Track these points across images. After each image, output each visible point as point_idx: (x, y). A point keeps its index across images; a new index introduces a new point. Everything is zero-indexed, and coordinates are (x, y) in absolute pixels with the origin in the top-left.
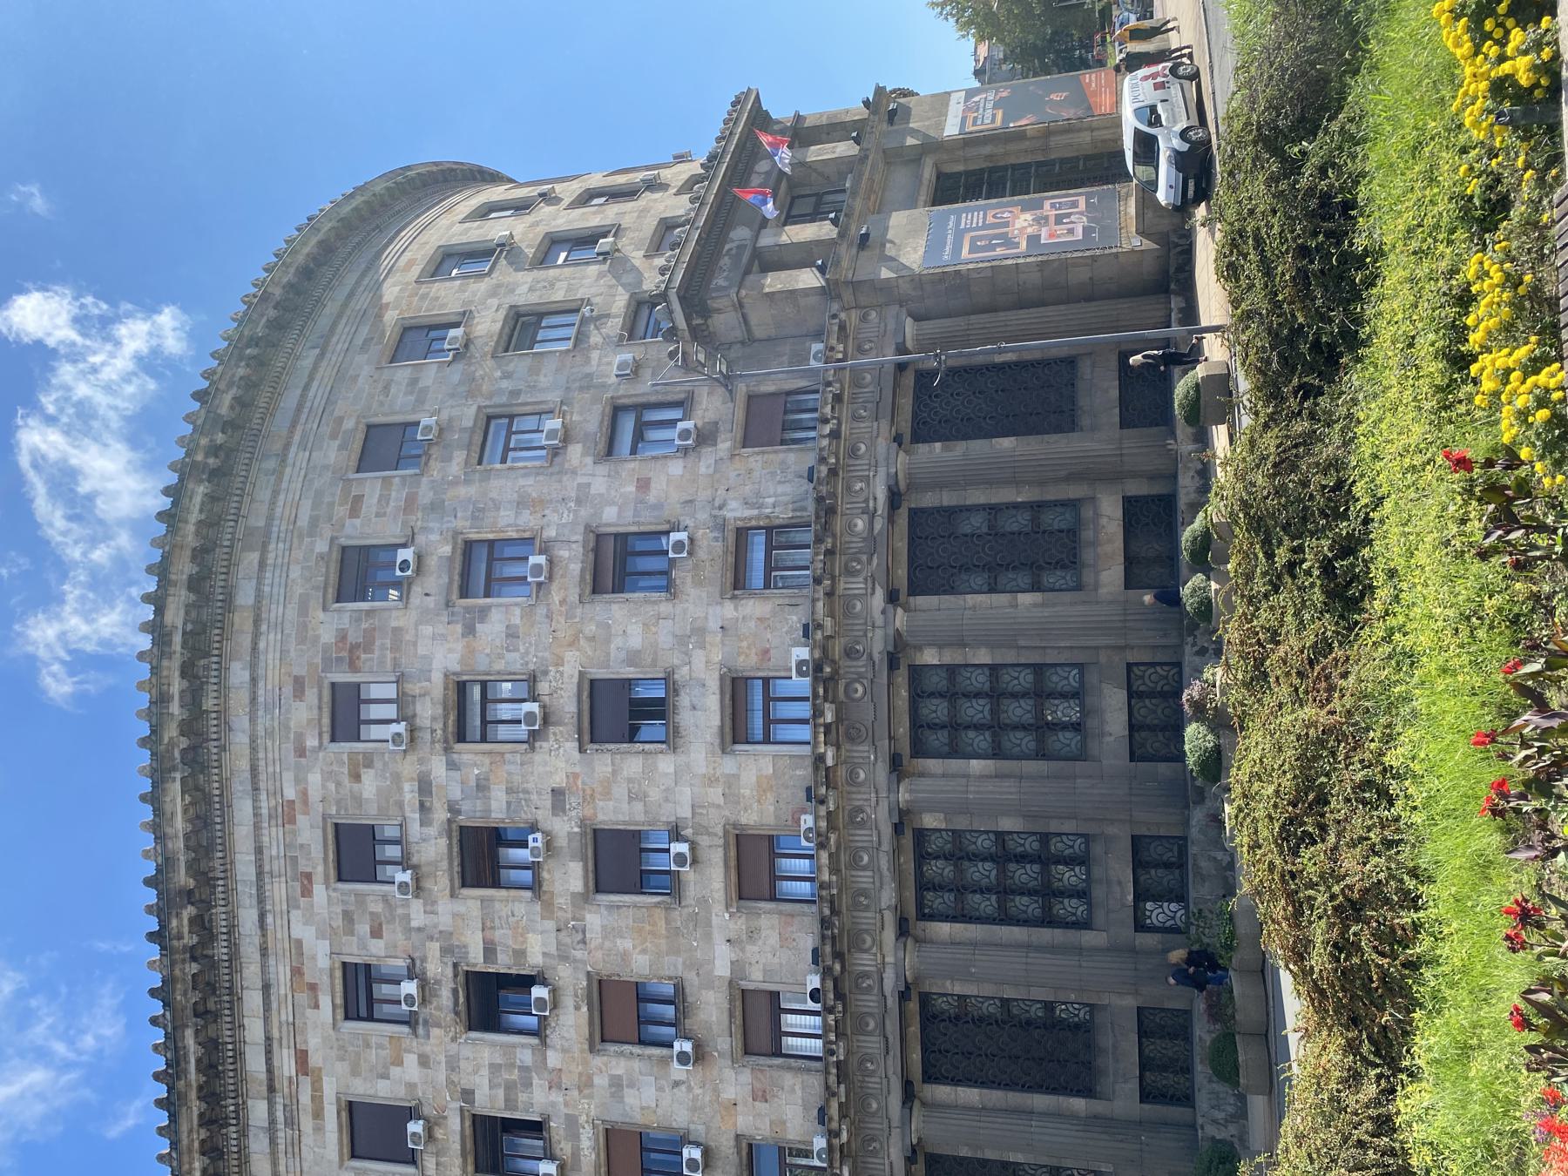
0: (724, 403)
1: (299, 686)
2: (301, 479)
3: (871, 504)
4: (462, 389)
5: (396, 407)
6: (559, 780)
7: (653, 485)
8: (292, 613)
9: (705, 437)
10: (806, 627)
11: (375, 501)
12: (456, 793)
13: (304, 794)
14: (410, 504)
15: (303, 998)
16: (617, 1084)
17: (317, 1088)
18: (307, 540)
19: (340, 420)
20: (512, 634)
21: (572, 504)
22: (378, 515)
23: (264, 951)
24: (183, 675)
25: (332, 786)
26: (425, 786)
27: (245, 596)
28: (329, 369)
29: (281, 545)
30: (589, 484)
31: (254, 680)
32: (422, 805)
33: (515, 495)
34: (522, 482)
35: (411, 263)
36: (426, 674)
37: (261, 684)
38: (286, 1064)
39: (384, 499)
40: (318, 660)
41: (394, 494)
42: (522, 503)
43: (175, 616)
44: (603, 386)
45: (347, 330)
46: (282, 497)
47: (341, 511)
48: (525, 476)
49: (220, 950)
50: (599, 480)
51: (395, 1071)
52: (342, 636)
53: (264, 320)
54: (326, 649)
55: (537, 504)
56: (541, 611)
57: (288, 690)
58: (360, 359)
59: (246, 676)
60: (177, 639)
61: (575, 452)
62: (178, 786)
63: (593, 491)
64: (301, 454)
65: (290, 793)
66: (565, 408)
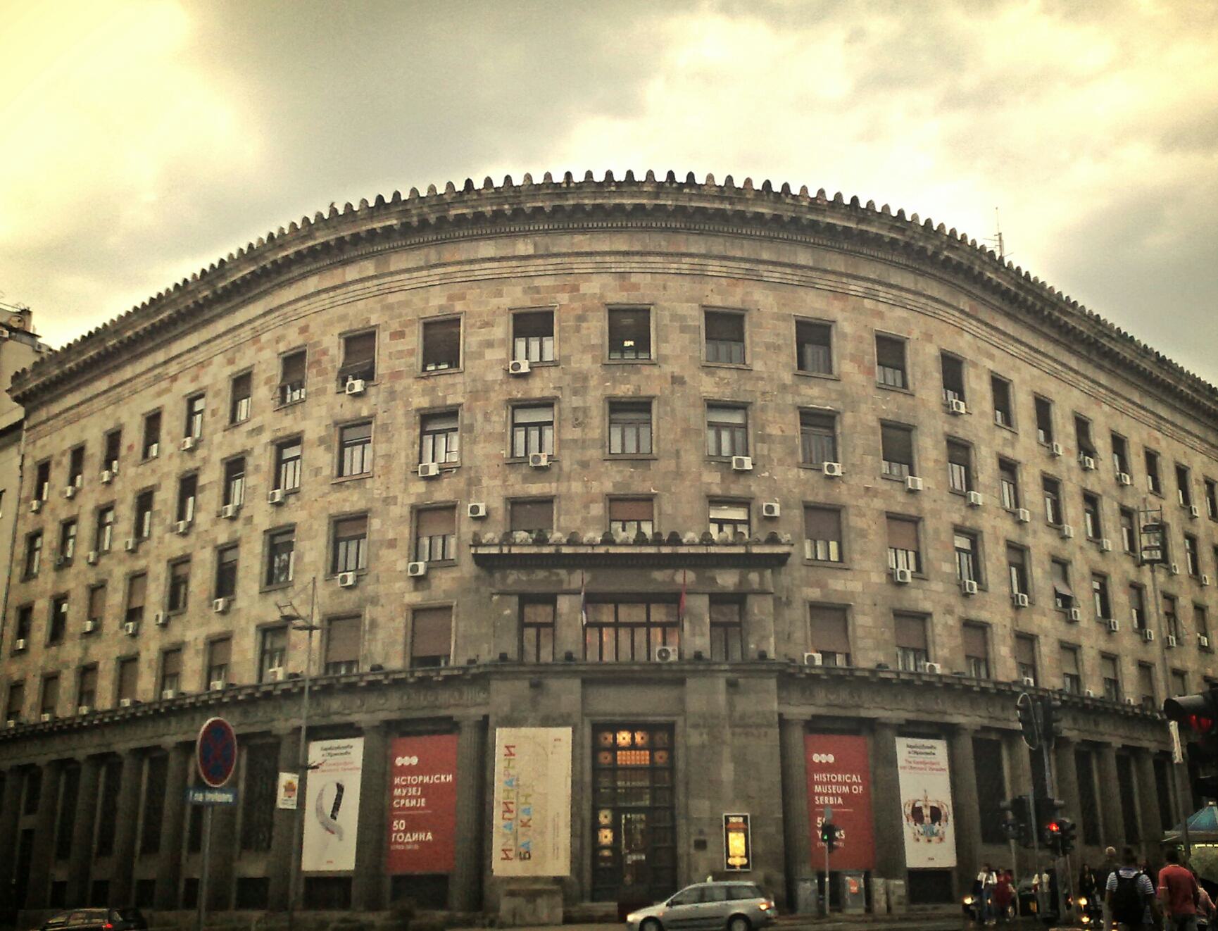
0: (444, 591)
1: (304, 330)
2: (419, 285)
3: (347, 712)
4: (479, 386)
5: (469, 340)
6: (256, 520)
7: (391, 551)
8: (340, 310)
9: (419, 582)
10: (296, 675)
11: (400, 348)
12: (256, 452)
13: (260, 350)
14: (396, 375)
15: (193, 371)
16: (157, 578)
17: (168, 390)
18: (378, 306)
19: (462, 297)
20: (317, 471)
21: (384, 495)
22: (390, 353)
23: (208, 342)
24: (298, 253)
25: (264, 366)
26: (259, 430)
27: (351, 273)
28: (511, 270)
29: (376, 288)
30: (396, 504)
31: (306, 297)
32: (253, 430)
33: (394, 451)
34: (403, 454)
35: (635, 287)
36: (304, 419)
37: (305, 302)
38: (173, 369)
39: (400, 355)
40: (316, 339)
41: (403, 360)
42: (388, 457)
43: (321, 238)
44: (469, 494)
45: (551, 267)
46: (407, 276)
47: (395, 326)
48: (407, 456)
49: (207, 315)
50: (400, 510)
51: (169, 438)
52: (325, 352)
53: (541, 205)
54: (318, 343)
55: (387, 470)
56: (326, 488)
57: (302, 322)
58: (518, 291)
59: (312, 290)
60: (311, 243)
61: (420, 487)
62: (252, 269)
63: (392, 507)
64: (437, 278)
65: (264, 338)
66: (455, 470)
